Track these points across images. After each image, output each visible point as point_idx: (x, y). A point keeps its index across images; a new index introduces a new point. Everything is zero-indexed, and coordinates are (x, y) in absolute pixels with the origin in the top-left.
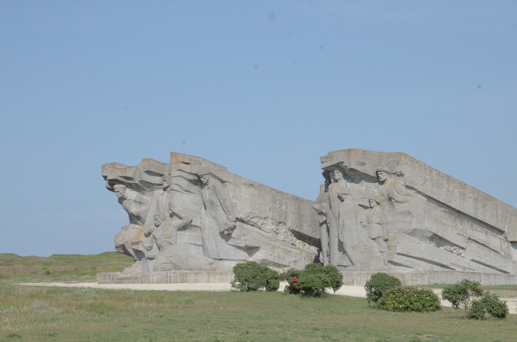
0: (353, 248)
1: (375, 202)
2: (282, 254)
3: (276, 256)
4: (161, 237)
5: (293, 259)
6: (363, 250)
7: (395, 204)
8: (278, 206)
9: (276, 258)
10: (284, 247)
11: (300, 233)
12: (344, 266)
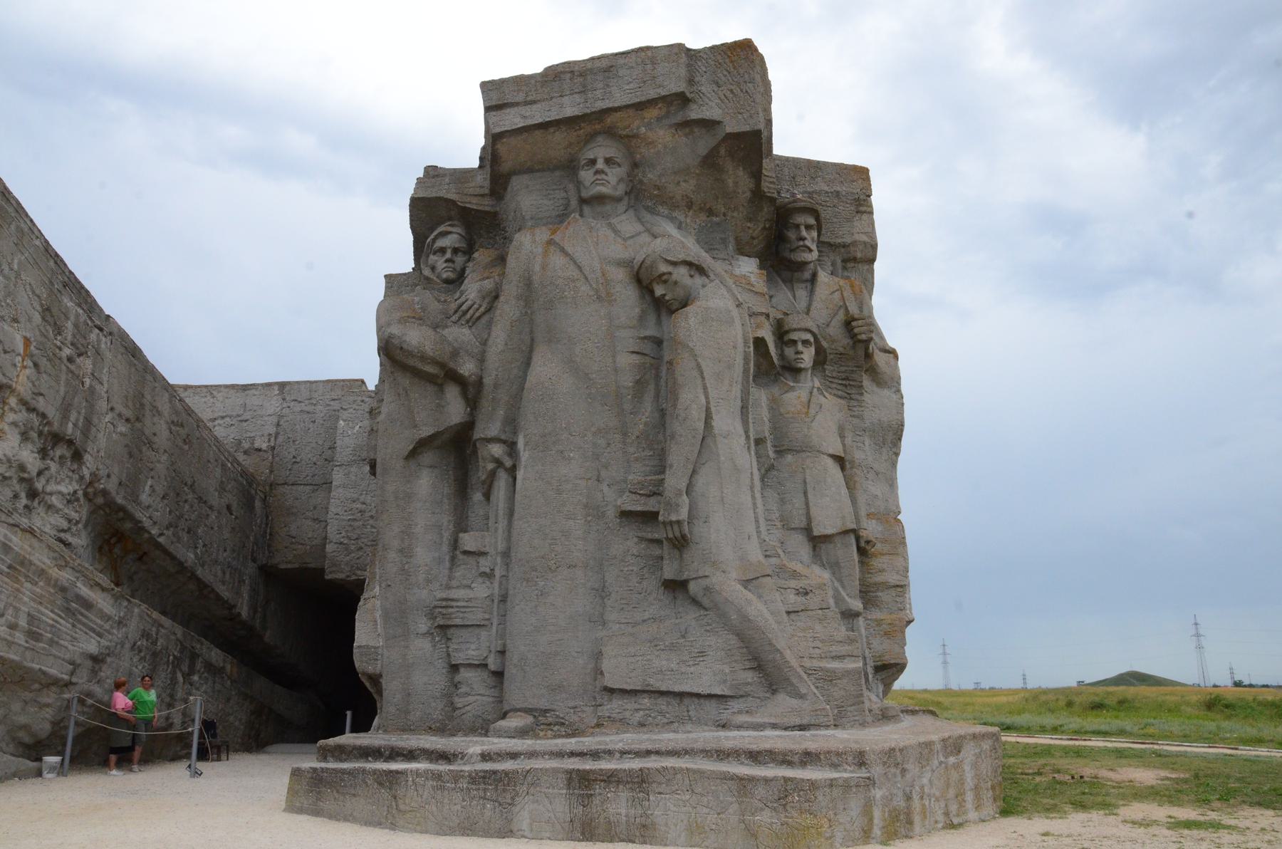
0: (746, 583)
1: (813, 350)
2: (48, 616)
3: (23, 622)
5: (92, 647)
6: (792, 597)
7: (867, 382)
8: (67, 351)
9: (20, 638)
10: (65, 576)
11: (129, 516)
12: (681, 695)
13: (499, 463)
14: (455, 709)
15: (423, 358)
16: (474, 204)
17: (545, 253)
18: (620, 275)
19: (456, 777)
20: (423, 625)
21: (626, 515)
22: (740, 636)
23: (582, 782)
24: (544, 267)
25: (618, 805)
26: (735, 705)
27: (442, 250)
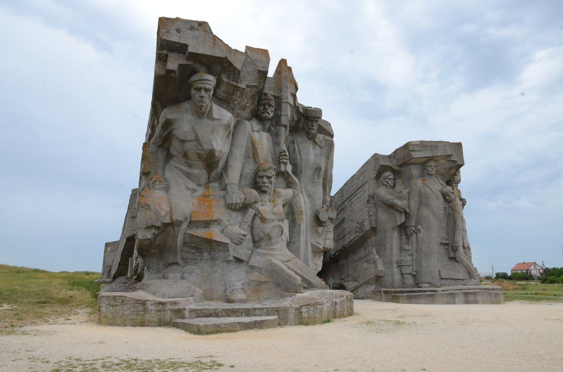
4: (274, 217)
12: (456, 279)
13: (414, 231)
14: (404, 283)
15: (401, 208)
16: (396, 168)
17: (424, 187)
18: (440, 194)
19: (445, 294)
20: (395, 265)
21: (442, 244)
22: (466, 268)
23: (466, 294)
24: (424, 190)
25: (472, 298)
26: (465, 281)
27: (390, 179)
